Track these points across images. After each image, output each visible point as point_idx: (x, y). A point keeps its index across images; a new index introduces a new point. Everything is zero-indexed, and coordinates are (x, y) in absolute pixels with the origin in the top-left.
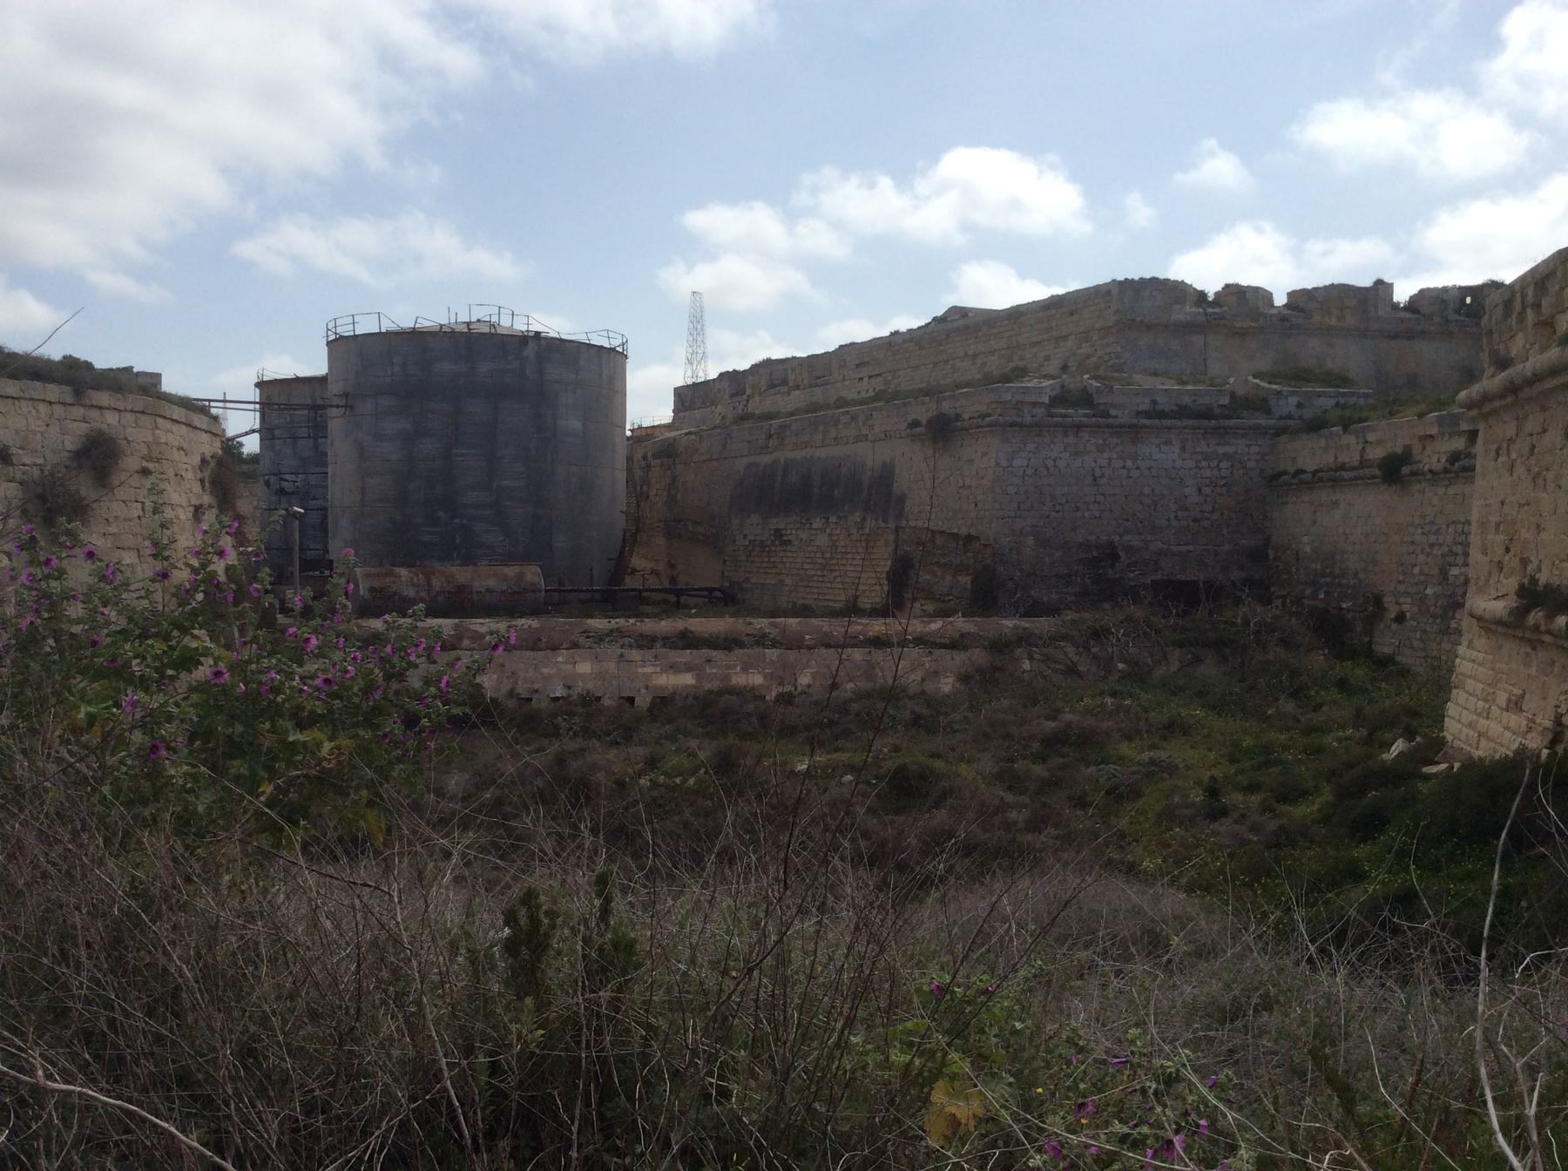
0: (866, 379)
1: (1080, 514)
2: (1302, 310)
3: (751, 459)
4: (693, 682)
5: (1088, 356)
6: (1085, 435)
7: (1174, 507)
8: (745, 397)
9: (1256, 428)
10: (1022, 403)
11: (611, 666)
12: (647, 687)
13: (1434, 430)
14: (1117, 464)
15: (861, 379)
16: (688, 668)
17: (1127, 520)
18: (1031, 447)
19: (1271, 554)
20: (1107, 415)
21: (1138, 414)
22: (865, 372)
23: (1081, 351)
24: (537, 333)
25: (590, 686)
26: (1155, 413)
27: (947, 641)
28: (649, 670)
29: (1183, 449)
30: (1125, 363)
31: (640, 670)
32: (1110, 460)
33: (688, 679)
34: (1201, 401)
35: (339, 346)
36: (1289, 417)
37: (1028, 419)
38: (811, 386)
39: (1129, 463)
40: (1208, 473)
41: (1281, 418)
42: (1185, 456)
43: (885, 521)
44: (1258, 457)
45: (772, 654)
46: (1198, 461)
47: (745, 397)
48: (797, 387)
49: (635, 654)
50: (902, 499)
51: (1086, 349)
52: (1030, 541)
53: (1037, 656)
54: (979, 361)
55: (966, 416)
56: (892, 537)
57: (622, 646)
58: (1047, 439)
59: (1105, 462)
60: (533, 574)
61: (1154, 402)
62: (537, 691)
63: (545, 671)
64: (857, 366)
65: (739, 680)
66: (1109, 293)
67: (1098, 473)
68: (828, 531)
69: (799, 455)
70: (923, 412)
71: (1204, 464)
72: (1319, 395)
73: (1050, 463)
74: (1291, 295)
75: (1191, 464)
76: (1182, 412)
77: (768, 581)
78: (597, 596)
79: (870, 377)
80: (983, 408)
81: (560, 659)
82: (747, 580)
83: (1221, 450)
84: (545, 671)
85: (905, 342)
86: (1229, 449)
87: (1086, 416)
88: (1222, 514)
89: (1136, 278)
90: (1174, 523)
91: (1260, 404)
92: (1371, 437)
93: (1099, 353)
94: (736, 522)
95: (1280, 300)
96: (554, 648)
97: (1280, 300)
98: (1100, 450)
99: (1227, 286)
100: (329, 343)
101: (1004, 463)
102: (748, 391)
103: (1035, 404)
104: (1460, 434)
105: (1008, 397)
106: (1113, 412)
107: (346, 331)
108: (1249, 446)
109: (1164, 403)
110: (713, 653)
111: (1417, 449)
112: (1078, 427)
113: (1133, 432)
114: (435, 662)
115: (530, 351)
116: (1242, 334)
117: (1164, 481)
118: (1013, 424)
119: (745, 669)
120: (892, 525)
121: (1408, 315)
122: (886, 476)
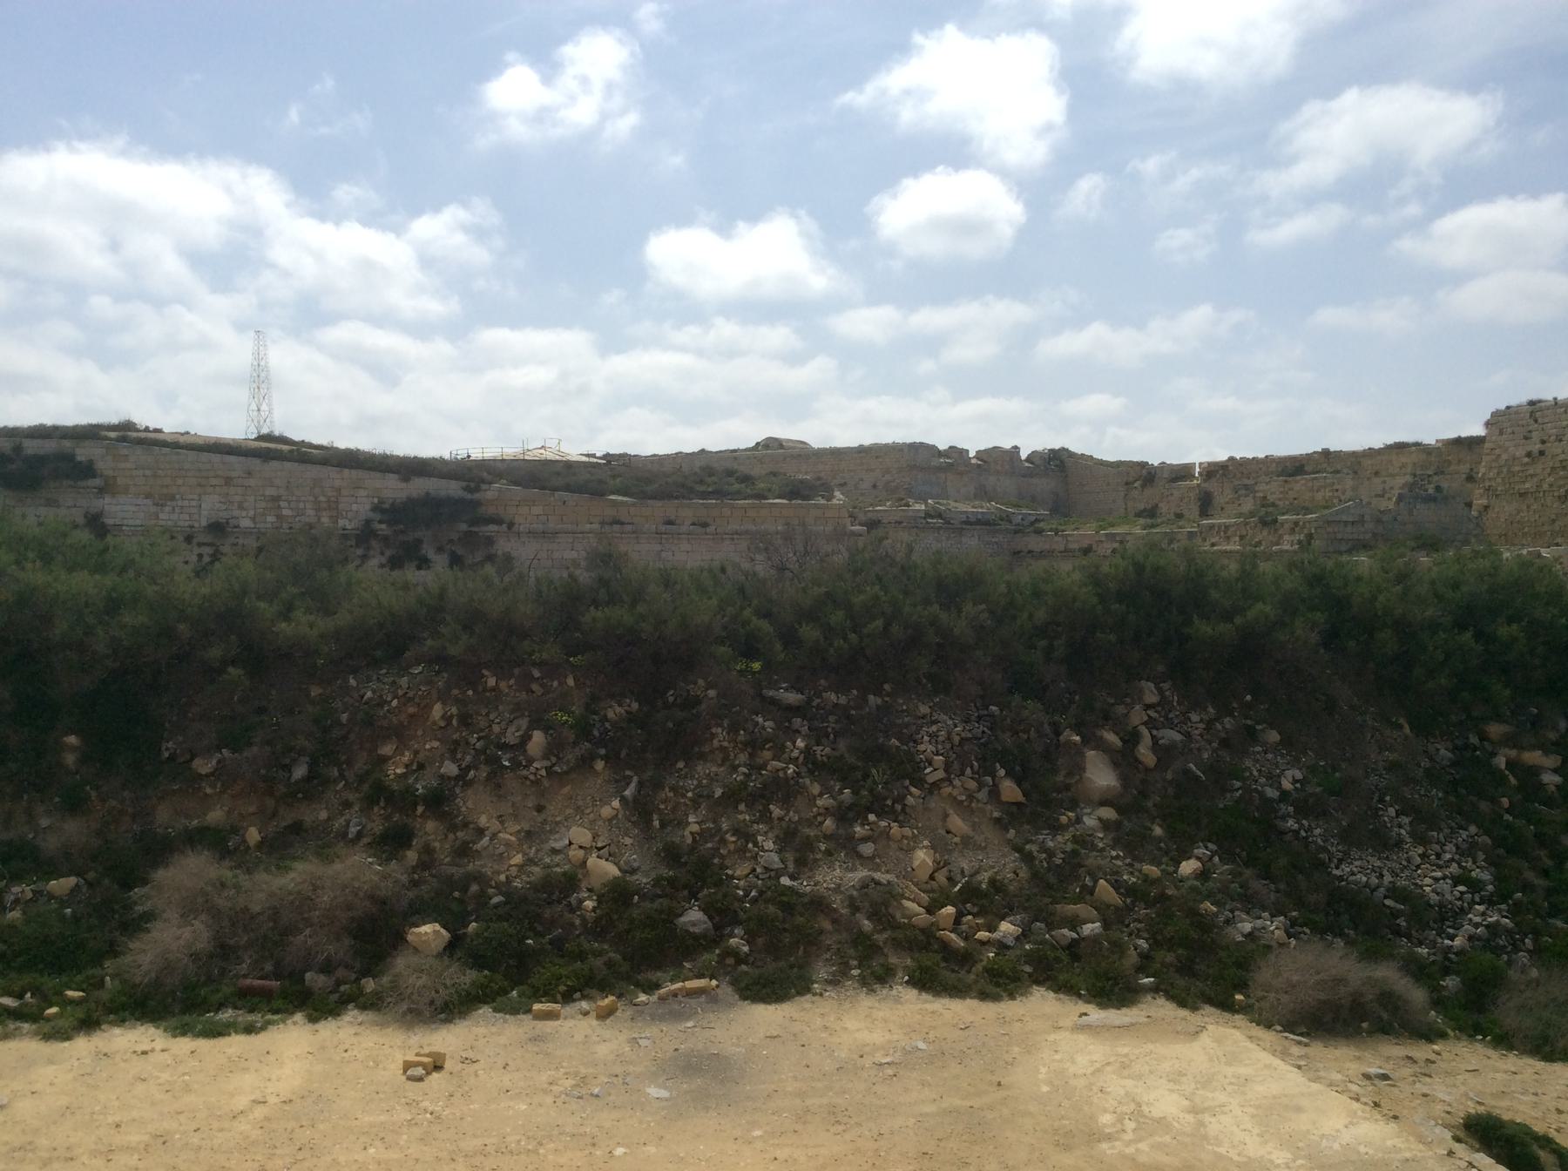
2: (985, 462)
6: (941, 532)
13: (1103, 539)
20: (950, 523)
23: (884, 479)
26: (967, 522)
32: (951, 544)
36: (1019, 525)
51: (888, 477)
61: (968, 517)
72: (1030, 514)
73: (928, 545)
74: (977, 452)
76: (979, 522)
83: (993, 540)
86: (997, 540)
92: (1069, 539)
95: (972, 454)
97: (972, 454)
98: (948, 539)
104: (1117, 542)
106: (952, 522)
109: (973, 519)
111: (1094, 547)
116: (961, 474)
121: (1027, 464)
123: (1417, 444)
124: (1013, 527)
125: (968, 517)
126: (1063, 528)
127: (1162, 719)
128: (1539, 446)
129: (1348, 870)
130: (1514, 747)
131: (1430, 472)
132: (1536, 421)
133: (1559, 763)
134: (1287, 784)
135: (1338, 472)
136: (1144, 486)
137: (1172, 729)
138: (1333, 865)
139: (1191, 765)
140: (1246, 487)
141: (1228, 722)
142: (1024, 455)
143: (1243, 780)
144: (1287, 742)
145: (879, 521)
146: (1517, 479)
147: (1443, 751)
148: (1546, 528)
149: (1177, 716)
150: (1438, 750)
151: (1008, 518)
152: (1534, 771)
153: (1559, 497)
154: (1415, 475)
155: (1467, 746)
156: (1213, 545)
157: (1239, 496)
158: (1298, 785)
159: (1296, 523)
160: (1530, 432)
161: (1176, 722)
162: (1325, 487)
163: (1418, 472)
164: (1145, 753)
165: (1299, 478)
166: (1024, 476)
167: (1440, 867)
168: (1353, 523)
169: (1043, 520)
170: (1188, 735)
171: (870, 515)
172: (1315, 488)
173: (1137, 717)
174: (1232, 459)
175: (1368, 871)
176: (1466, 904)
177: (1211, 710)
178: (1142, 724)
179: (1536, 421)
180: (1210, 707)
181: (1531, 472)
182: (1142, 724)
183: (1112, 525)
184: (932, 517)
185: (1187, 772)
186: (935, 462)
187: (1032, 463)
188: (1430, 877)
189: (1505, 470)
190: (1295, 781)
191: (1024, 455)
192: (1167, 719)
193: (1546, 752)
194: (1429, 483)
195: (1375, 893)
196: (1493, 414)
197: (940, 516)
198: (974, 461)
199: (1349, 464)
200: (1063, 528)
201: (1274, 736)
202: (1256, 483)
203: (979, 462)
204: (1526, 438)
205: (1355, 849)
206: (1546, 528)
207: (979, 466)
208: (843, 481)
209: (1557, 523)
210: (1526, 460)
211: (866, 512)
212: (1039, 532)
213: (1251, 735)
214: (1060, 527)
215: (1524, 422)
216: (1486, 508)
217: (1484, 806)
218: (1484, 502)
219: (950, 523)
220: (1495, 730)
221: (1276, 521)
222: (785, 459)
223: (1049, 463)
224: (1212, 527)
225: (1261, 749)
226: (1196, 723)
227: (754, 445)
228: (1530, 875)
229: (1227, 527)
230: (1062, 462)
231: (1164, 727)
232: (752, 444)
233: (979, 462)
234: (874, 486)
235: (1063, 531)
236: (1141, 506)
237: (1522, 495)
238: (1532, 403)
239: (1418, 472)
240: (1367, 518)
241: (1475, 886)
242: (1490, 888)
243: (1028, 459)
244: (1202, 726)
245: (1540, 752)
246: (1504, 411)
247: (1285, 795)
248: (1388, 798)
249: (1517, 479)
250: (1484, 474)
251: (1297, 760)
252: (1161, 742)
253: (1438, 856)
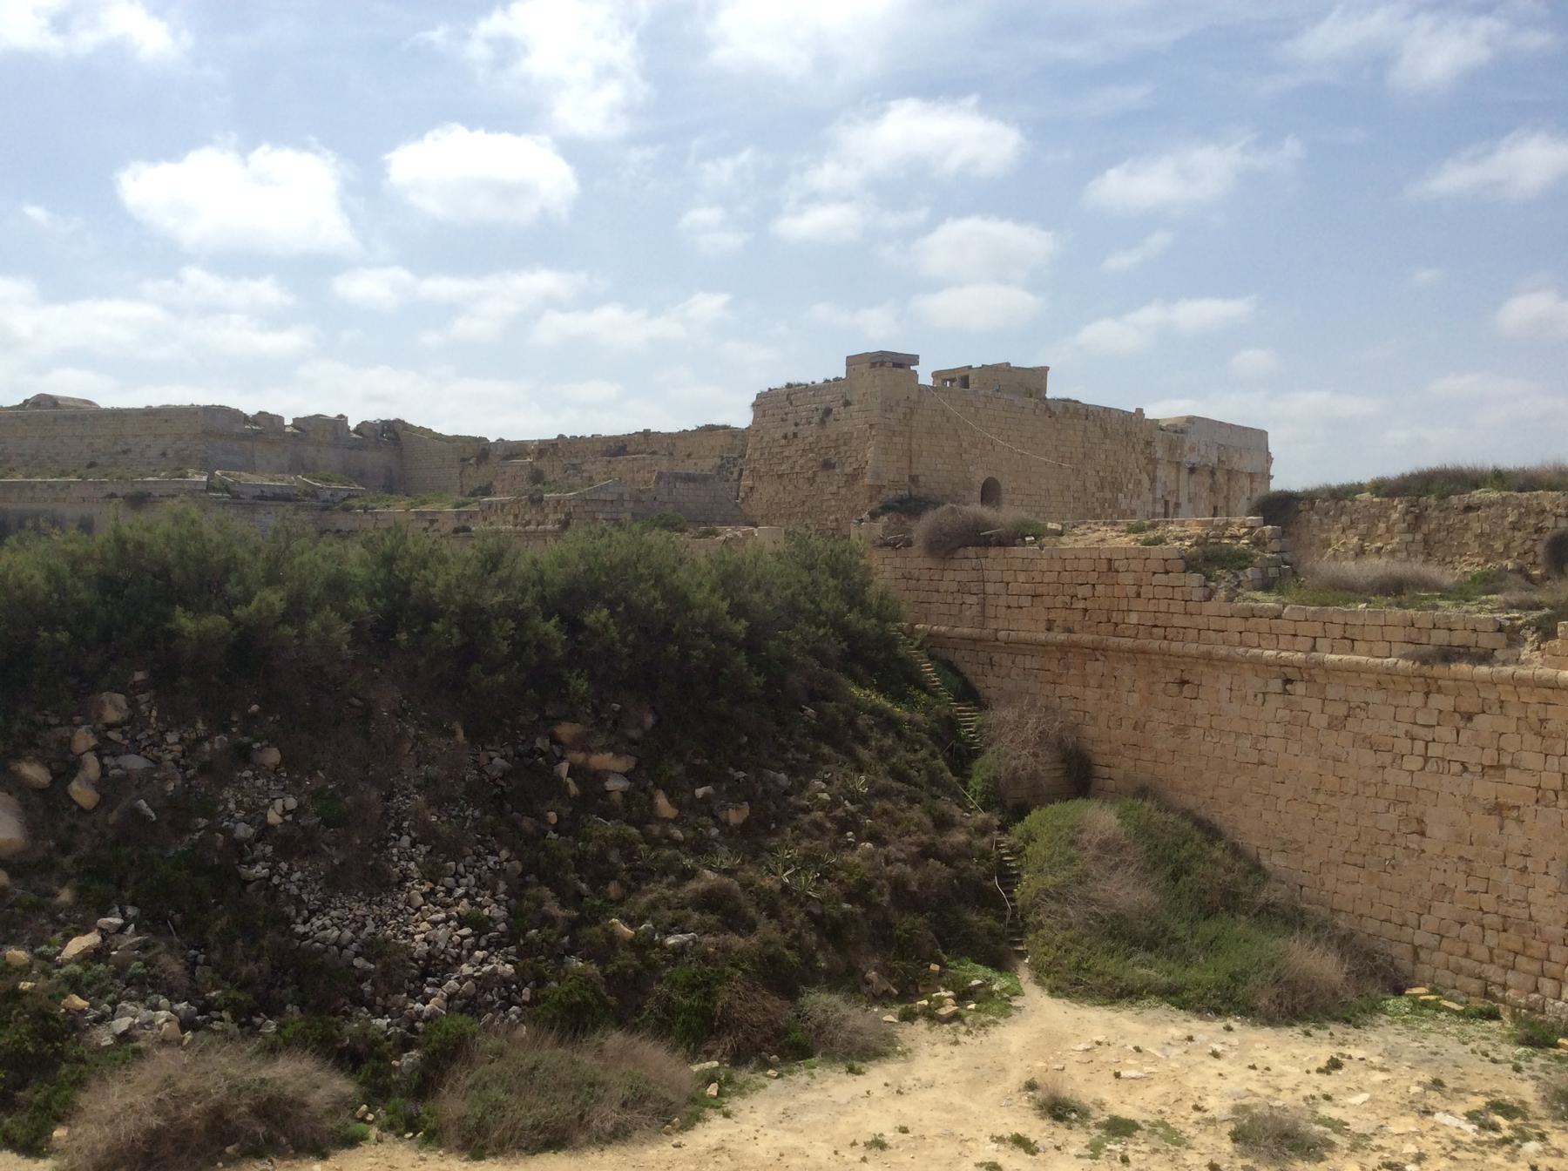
5: (182, 450)
20: (239, 498)
21: (254, 497)
26: (262, 497)
36: (327, 501)
41: (324, 501)
66: (196, 413)
72: (344, 490)
74: (294, 420)
95: (288, 422)
97: (288, 422)
99: (260, 413)
106: (242, 496)
112: (225, 503)
116: (272, 443)
121: (355, 436)
123: (725, 427)
124: (319, 504)
126: (374, 505)
127: (126, 742)
128: (793, 428)
129: (320, 923)
130: (583, 750)
131: (735, 455)
132: (791, 404)
133: (632, 766)
134: (273, 817)
135: (654, 453)
136: (479, 462)
137: (138, 754)
138: (299, 920)
139: (142, 802)
140: (574, 466)
141: (221, 740)
142: (352, 424)
143: (209, 813)
144: (288, 761)
145: (150, 494)
146: (776, 460)
147: (497, 760)
148: (797, 509)
149: (149, 736)
150: (491, 759)
151: (314, 494)
152: (599, 776)
153: (808, 478)
154: (722, 459)
155: (533, 752)
156: (491, 524)
157: (569, 475)
158: (289, 818)
159: (558, 502)
160: (786, 414)
161: (144, 743)
162: (644, 468)
163: (725, 455)
164: (82, 792)
165: (621, 457)
166: (351, 448)
167: (446, 906)
168: (612, 501)
169: (357, 497)
170: (157, 761)
171: (139, 487)
172: (636, 469)
173: (83, 739)
174: (561, 437)
175: (347, 922)
176: (464, 952)
177: (200, 725)
178: (89, 750)
179: (791, 404)
180: (200, 721)
181: (786, 454)
182: (89, 750)
183: (424, 503)
184: (215, 490)
185: (136, 811)
186: (237, 429)
187: (361, 434)
188: (428, 922)
189: (766, 452)
190: (285, 812)
191: (352, 424)
192: (134, 741)
193: (618, 754)
194: (735, 466)
195: (345, 950)
196: (759, 396)
197: (228, 490)
198: (288, 430)
199: (665, 445)
200: (374, 505)
201: (273, 756)
202: (583, 463)
203: (295, 431)
204: (783, 420)
205: (341, 894)
206: (797, 509)
207: (294, 435)
208: (126, 448)
209: (808, 504)
210: (783, 442)
211: (133, 484)
212: (347, 509)
213: (243, 755)
214: (371, 505)
215: (782, 404)
216: (752, 488)
217: (527, 824)
218: (750, 483)
219: (239, 498)
220: (566, 731)
221: (541, 499)
222: (55, 420)
223: (382, 435)
224: (490, 505)
225: (251, 773)
226: (171, 745)
227: (22, 402)
228: (553, 908)
229: (503, 505)
230: (396, 434)
231: (128, 752)
232: (19, 401)
233: (295, 431)
234: (164, 454)
235: (373, 509)
236: (476, 485)
237: (780, 476)
238: (789, 386)
239: (725, 455)
240: (626, 497)
241: (480, 925)
242: (502, 927)
243: (357, 431)
244: (179, 748)
245: (611, 754)
246: (767, 393)
247: (265, 831)
248: (406, 824)
249: (776, 460)
250: (750, 455)
251: (298, 784)
252: (111, 773)
253: (449, 892)
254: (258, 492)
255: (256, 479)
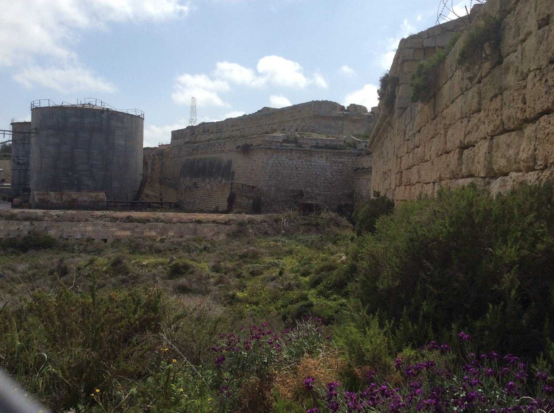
0: (234, 131)
1: (291, 180)
3: (188, 157)
4: (130, 234)
5: (304, 126)
6: (294, 153)
7: (323, 179)
8: (195, 136)
9: (350, 153)
10: (272, 141)
11: (100, 228)
12: (112, 236)
14: (304, 163)
15: (233, 131)
16: (129, 229)
17: (307, 183)
18: (275, 156)
19: (354, 196)
20: (301, 147)
21: (312, 147)
22: (234, 128)
24: (108, 109)
25: (91, 235)
26: (317, 147)
27: (223, 222)
28: (114, 229)
29: (327, 159)
30: (316, 129)
31: (111, 230)
32: (302, 162)
33: (128, 233)
34: (333, 143)
35: (36, 111)
36: (362, 150)
37: (274, 147)
38: (217, 133)
39: (308, 163)
40: (334, 168)
41: (359, 150)
42: (327, 161)
43: (228, 181)
44: (352, 163)
45: (161, 225)
46: (331, 164)
47: (195, 136)
48: (212, 133)
49: (109, 224)
50: (233, 173)
52: (273, 188)
53: (254, 228)
54: (270, 126)
55: (254, 145)
56: (230, 186)
57: (105, 221)
58: (281, 154)
59: (300, 163)
60: (102, 196)
61: (317, 143)
62: (70, 236)
63: (74, 229)
64: (232, 126)
65: (147, 233)
66: (311, 105)
67: (298, 166)
68: (211, 183)
69: (203, 156)
70: (241, 143)
71: (334, 164)
73: (281, 162)
74: (372, 108)
75: (329, 164)
76: (327, 147)
77: (191, 201)
78: (129, 204)
79: (236, 130)
80: (260, 143)
81: (81, 225)
82: (185, 199)
83: (339, 160)
84: (74, 229)
85: (247, 118)
86: (342, 160)
87: (294, 146)
88: (339, 182)
89: (321, 101)
90: (323, 184)
91: (353, 145)
93: (307, 126)
94: (182, 179)
96: (79, 221)
97: (369, 110)
98: (299, 158)
99: (351, 105)
100: (32, 110)
101: (265, 161)
102: (196, 134)
103: (277, 142)
105: (267, 139)
106: (303, 146)
107: (37, 105)
108: (349, 159)
109: (321, 144)
110: (139, 224)
112: (291, 150)
113: (310, 153)
114: (33, 225)
115: (105, 115)
116: (355, 121)
117: (320, 170)
118: (269, 148)
119: (150, 230)
120: (230, 182)
122: (229, 164)
124: (356, 151)
125: (317, 143)
184: (290, 142)
254: (314, 143)
255: (315, 136)
